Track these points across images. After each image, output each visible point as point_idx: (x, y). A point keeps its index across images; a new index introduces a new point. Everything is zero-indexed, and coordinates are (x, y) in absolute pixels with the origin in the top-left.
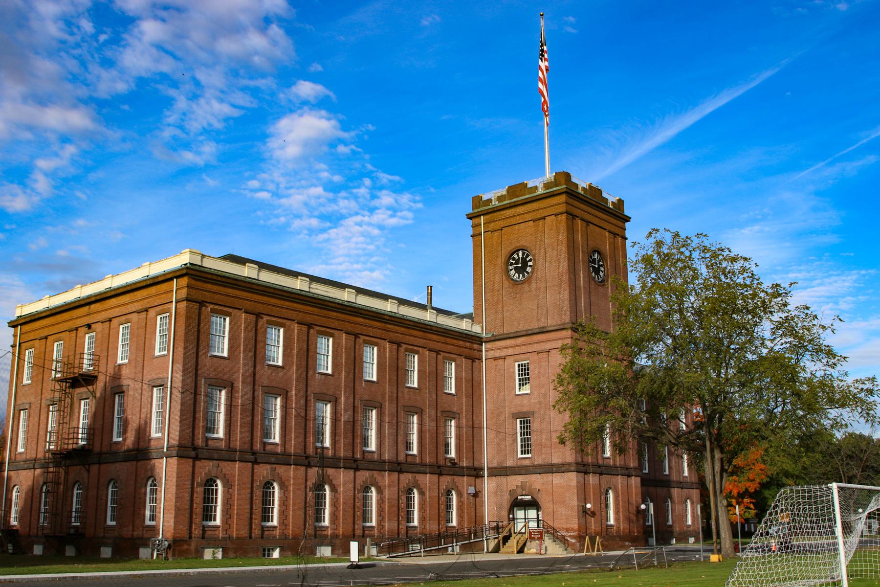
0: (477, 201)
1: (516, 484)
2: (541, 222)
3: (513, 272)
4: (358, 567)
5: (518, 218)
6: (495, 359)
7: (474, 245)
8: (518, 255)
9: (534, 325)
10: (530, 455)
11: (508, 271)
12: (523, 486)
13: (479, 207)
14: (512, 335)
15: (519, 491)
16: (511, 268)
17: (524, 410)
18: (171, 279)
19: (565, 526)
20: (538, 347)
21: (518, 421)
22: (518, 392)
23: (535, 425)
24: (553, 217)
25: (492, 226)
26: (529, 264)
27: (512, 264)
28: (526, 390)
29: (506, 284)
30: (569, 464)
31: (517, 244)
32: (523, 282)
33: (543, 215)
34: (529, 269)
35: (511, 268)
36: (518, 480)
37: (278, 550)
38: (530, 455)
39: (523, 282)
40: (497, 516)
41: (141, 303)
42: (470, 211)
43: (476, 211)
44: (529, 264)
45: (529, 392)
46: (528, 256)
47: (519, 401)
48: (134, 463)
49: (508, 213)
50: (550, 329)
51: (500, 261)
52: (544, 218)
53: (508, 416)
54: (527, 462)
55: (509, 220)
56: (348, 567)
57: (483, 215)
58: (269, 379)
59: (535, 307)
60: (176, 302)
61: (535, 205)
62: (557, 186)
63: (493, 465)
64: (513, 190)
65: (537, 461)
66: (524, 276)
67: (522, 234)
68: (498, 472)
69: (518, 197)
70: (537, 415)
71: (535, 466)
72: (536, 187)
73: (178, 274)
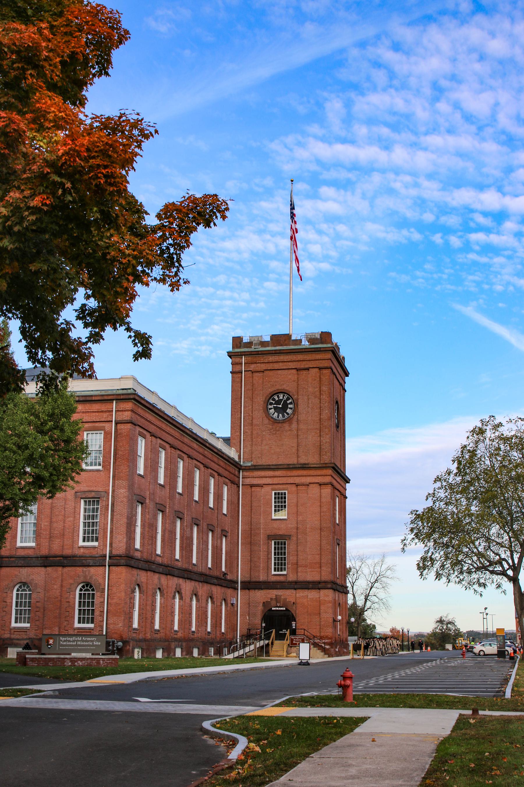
0: (237, 341)
1: (269, 596)
2: (304, 372)
3: (272, 411)
4: (307, 664)
5: (281, 364)
6: (252, 486)
7: (233, 381)
8: (278, 397)
9: (293, 461)
10: (284, 573)
11: (267, 410)
12: (277, 599)
13: (240, 347)
14: (273, 467)
15: (273, 603)
16: (270, 407)
17: (281, 533)
19: (318, 635)
20: (298, 480)
21: (273, 542)
22: (274, 517)
23: (290, 547)
24: (317, 370)
25: (252, 367)
26: (289, 406)
28: (283, 515)
29: (266, 421)
30: (325, 582)
31: (279, 387)
32: (284, 422)
33: (307, 366)
34: (289, 411)
35: (270, 407)
36: (274, 593)
37: (161, 650)
38: (284, 573)
39: (284, 422)
40: (249, 625)
42: (231, 349)
44: (289, 406)
45: (286, 517)
46: (288, 399)
47: (276, 525)
48: (60, 569)
49: (271, 358)
50: (312, 466)
51: (260, 400)
52: (308, 369)
53: (262, 537)
54: (282, 579)
55: (271, 365)
56: (300, 664)
57: (244, 355)
58: (159, 497)
59: (295, 445)
60: (117, 423)
61: (300, 357)
62: (322, 343)
63: (247, 579)
64: (276, 339)
65: (292, 578)
66: (283, 416)
67: (286, 380)
68: (248, 586)
69: (281, 345)
70: (294, 538)
71: (290, 583)
72: (301, 341)
73: (119, 397)
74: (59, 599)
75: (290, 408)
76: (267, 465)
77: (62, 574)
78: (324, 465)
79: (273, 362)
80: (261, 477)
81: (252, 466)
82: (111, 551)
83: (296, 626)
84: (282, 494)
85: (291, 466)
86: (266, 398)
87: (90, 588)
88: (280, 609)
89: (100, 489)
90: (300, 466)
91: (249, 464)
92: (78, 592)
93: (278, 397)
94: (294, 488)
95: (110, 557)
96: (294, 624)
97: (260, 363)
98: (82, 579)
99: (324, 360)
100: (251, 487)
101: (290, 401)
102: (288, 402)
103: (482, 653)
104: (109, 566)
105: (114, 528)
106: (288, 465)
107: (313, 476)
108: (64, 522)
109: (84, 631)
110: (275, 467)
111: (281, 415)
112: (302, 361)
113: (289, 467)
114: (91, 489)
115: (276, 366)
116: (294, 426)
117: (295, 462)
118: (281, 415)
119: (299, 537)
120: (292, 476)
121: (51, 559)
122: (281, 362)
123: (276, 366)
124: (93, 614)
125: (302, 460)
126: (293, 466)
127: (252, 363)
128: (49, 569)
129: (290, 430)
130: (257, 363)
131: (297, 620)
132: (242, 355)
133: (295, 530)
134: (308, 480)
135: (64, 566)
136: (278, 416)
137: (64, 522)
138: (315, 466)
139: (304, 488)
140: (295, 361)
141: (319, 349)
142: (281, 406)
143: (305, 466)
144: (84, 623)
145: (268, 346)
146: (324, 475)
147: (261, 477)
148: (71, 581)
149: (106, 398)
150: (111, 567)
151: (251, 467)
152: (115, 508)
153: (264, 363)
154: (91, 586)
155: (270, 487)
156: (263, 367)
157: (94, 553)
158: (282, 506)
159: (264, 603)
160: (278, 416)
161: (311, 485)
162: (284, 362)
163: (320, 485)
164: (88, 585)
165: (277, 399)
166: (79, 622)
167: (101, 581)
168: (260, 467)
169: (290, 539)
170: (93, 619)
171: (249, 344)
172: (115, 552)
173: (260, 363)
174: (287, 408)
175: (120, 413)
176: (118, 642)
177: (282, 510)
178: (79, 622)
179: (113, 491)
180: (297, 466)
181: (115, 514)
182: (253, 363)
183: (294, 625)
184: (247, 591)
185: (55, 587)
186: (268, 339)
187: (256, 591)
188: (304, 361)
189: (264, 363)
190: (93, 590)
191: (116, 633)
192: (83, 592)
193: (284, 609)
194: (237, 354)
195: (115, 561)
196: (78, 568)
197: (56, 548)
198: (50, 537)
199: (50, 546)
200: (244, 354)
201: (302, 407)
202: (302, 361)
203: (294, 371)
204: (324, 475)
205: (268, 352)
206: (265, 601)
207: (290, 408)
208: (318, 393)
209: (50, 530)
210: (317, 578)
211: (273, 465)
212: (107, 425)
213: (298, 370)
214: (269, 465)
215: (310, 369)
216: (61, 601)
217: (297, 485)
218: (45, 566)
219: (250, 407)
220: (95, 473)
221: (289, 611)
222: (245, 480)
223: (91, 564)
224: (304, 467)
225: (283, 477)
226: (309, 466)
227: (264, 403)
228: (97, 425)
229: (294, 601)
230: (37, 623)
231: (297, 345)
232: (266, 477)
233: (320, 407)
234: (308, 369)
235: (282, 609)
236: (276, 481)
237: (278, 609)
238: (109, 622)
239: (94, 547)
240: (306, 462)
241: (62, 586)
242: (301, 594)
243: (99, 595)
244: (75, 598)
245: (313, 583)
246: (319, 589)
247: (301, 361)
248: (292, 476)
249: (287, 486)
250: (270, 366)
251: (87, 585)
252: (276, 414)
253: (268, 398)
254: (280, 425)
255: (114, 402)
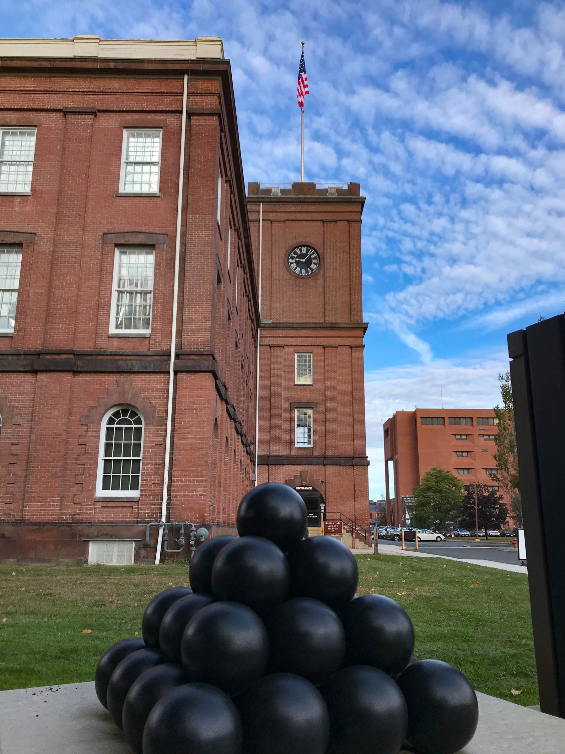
2: (331, 224)
3: (294, 265)
5: (304, 214)
6: (270, 347)
8: (301, 251)
9: (319, 319)
11: (287, 264)
12: (302, 476)
13: (257, 194)
14: (297, 326)
16: (291, 261)
18: (180, 73)
20: (325, 342)
22: (296, 383)
24: (346, 223)
25: (271, 216)
26: (314, 261)
27: (293, 258)
29: (287, 276)
33: (335, 218)
34: (313, 266)
39: (308, 277)
41: (76, 98)
43: (252, 196)
45: (311, 383)
48: (68, 376)
49: (293, 208)
50: (342, 326)
51: (280, 252)
52: (335, 221)
53: (284, 406)
57: (262, 202)
60: (189, 115)
67: (310, 232)
71: (319, 457)
74: (64, 437)
75: (314, 263)
76: (290, 323)
77: (71, 388)
78: (357, 326)
79: (295, 212)
80: (282, 337)
81: (272, 323)
82: (179, 346)
83: (325, 509)
84: (306, 357)
85: (318, 326)
86: (287, 251)
87: (131, 416)
88: (305, 488)
89: (157, 230)
90: (328, 325)
91: (270, 322)
92: (104, 425)
93: (301, 251)
94: (321, 350)
95: (177, 356)
96: (322, 507)
97: (281, 212)
98: (115, 399)
99: (354, 212)
100: (270, 347)
101: (315, 255)
102: (312, 257)
103: (439, 539)
104: (176, 373)
105: (186, 301)
106: (315, 323)
107: (343, 337)
108: (79, 288)
109: (117, 504)
110: (300, 326)
111: (303, 270)
112: (329, 212)
113: (315, 327)
114: (137, 229)
115: (299, 216)
116: (320, 282)
117: (322, 321)
118: (303, 270)
119: (327, 405)
120: (319, 337)
121: (48, 357)
122: (304, 212)
123: (299, 216)
124: (136, 470)
125: (331, 319)
126: (321, 326)
127: (270, 212)
128: (43, 377)
129: (315, 287)
130: (277, 212)
131: (327, 502)
132: (260, 202)
133: (323, 398)
134: (338, 342)
135: (75, 373)
136: (301, 272)
137: (79, 288)
138: (346, 326)
139: (332, 350)
140: (321, 212)
141: (349, 200)
142: (304, 260)
143: (334, 326)
144: (115, 488)
145: (290, 195)
146: (356, 337)
147: (282, 337)
148: (91, 403)
149: (170, 67)
150: (180, 375)
151: (271, 325)
152: (188, 264)
153: (285, 212)
154: (134, 414)
155: (292, 349)
156: (284, 217)
157: (142, 348)
158: (306, 370)
159: (286, 481)
160: (301, 272)
161: (339, 347)
162: (309, 212)
163: (351, 347)
164: (126, 411)
165: (299, 253)
166: (105, 487)
167: (157, 402)
168: (281, 325)
169: (317, 407)
170: (135, 479)
171: (268, 191)
172: (187, 347)
173: (281, 212)
174: (312, 263)
175: (198, 99)
176: (198, 527)
177: (306, 375)
178: (105, 487)
179: (183, 234)
180: (326, 325)
181: (187, 275)
182: (272, 212)
183: (323, 508)
184: (266, 467)
185: (56, 413)
186: (290, 187)
187: (277, 466)
188: (331, 212)
189: (285, 212)
190: (139, 421)
191: (191, 509)
192: (115, 426)
193: (311, 488)
194: (255, 200)
195: (187, 363)
196: (107, 377)
197: (60, 337)
198: (48, 315)
199: (45, 334)
200: (262, 200)
201: (327, 263)
202: (329, 212)
203: (319, 223)
204: (356, 337)
205: (290, 200)
206: (287, 479)
207: (314, 263)
208: (347, 248)
209: (48, 301)
210: (349, 453)
211: (297, 323)
212: (170, 119)
213: (323, 221)
214: (293, 323)
215: (338, 222)
216: (67, 441)
217: (324, 347)
218: (35, 372)
219: (269, 260)
220: (146, 200)
221: (317, 491)
222: (264, 339)
223: (136, 369)
224: (333, 327)
225: (306, 337)
226: (339, 326)
227: (285, 255)
228: (150, 116)
229: (322, 478)
230: (11, 488)
231: (323, 195)
232: (289, 337)
233: (350, 263)
234: (335, 221)
235: (308, 488)
236: (299, 341)
237: (303, 488)
238: (174, 485)
239: (142, 338)
240: (335, 321)
241: (70, 412)
242: (331, 470)
243: (152, 431)
244: (98, 437)
245: (345, 457)
246: (353, 465)
247: (327, 212)
248: (319, 337)
249: (312, 348)
250: (292, 216)
251: (125, 412)
252: (298, 269)
253: (290, 251)
254: (303, 280)
255: (186, 78)
